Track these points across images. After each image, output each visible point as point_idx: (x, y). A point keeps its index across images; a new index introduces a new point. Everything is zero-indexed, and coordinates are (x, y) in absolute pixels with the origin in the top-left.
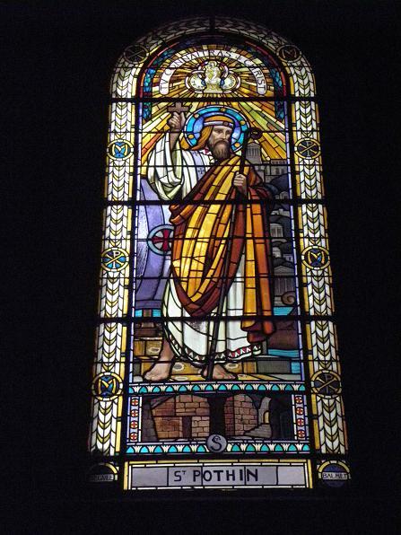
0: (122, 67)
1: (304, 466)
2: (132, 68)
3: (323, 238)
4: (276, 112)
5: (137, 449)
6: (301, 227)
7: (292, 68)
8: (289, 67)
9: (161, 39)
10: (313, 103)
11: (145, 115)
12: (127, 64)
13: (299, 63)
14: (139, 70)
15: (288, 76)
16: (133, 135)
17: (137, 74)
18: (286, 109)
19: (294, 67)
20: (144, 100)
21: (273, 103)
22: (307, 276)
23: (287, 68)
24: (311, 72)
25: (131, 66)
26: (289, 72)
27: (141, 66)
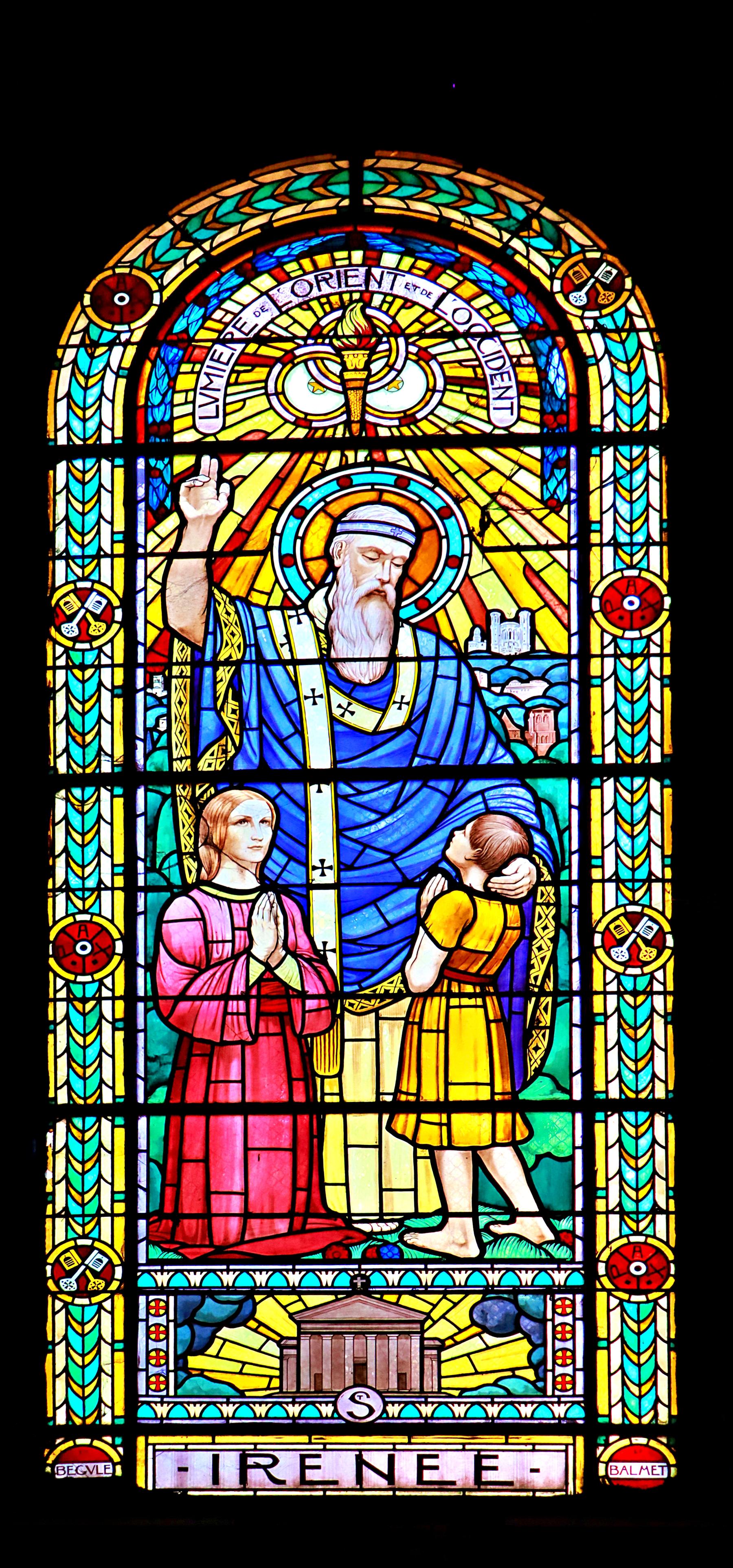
4: (544, 482)
5: (162, 1410)
7: (597, 337)
11: (154, 501)
15: (581, 363)
17: (127, 363)
18: (573, 474)
19: (604, 332)
20: (150, 452)
23: (583, 338)
26: (588, 351)
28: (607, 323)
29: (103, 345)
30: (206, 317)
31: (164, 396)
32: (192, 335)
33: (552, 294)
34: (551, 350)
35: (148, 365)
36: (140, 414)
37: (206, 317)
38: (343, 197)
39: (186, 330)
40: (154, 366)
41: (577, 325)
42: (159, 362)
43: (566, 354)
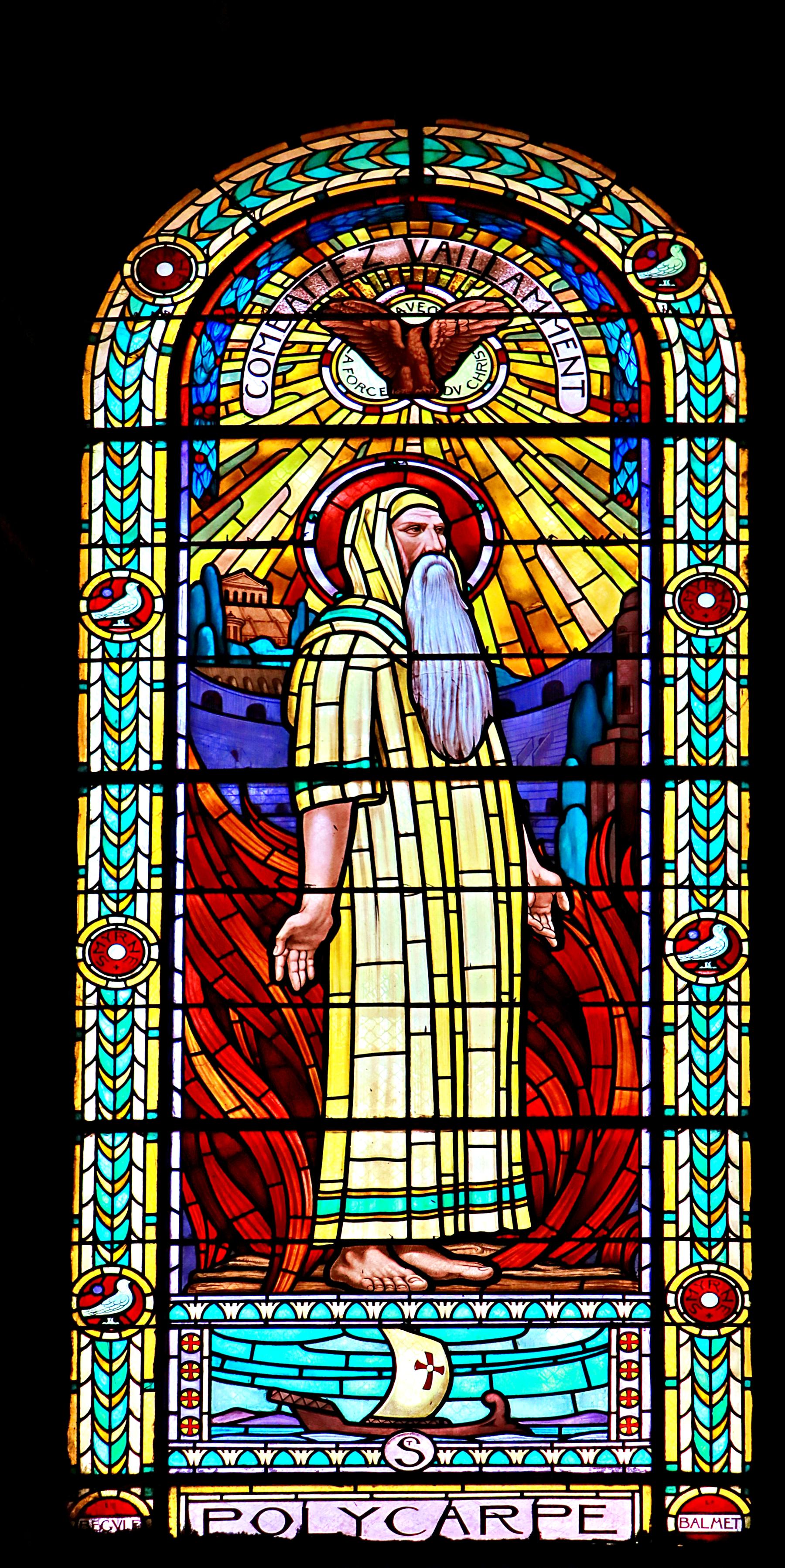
0: (122, 318)
1: (632, 1498)
2: (154, 318)
3: (735, 887)
6: (669, 854)
7: (670, 322)
8: (662, 316)
9: (246, 212)
10: (730, 446)
12: (135, 306)
13: (695, 302)
14: (175, 326)
16: (161, 553)
17: (170, 339)
19: (678, 316)
21: (605, 443)
22: (676, 1003)
23: (656, 322)
24: (733, 337)
25: (148, 311)
27: (182, 310)
28: (683, 308)
29: (146, 318)
30: (255, 291)
31: (210, 374)
32: (240, 310)
33: (624, 274)
34: (622, 334)
35: (193, 341)
36: (185, 392)
37: (255, 291)
38: (402, 168)
39: (234, 305)
40: (199, 342)
41: (651, 308)
42: (204, 338)
43: (638, 337)
